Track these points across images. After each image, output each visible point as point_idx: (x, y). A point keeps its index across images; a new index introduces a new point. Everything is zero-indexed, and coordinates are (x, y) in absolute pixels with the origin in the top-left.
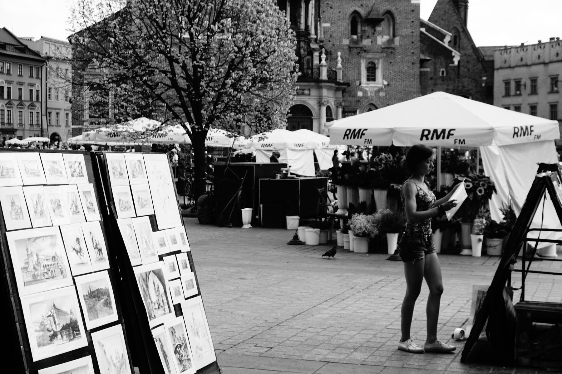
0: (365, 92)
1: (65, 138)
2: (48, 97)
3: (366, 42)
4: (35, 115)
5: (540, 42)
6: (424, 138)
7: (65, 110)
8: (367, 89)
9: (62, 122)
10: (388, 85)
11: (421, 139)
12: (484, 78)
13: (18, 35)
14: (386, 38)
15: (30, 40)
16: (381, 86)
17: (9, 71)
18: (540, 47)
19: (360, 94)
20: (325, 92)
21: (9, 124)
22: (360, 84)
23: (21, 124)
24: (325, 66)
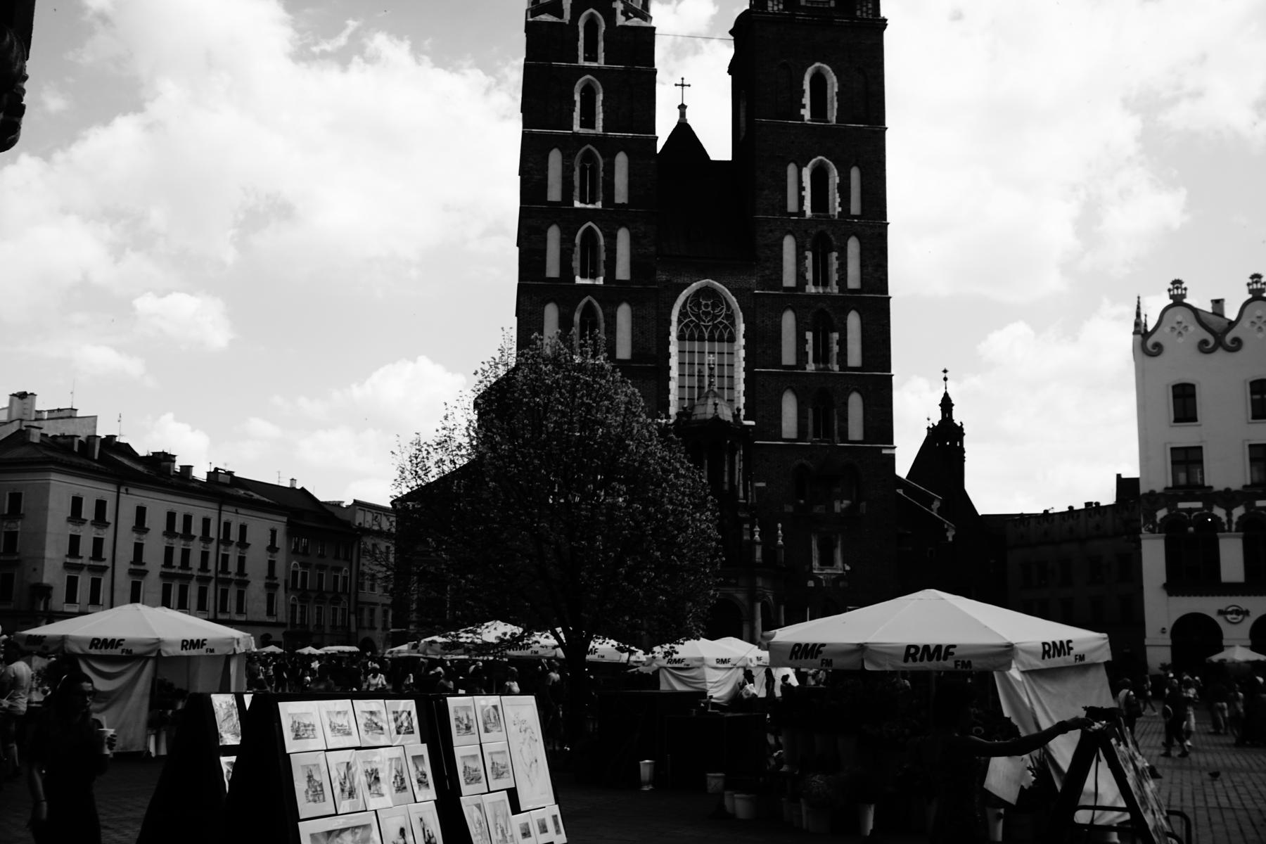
0: (817, 581)
1: (382, 646)
2: (360, 586)
3: (818, 509)
4: (339, 612)
5: (1071, 508)
6: (910, 659)
7: (383, 605)
8: (821, 577)
9: (379, 625)
11: (906, 660)
12: (992, 561)
13: (322, 496)
14: (846, 502)
15: (337, 505)
16: (840, 572)
17: (305, 548)
18: (1073, 517)
19: (811, 584)
20: (760, 582)
21: (302, 624)
22: (811, 568)
23: (319, 626)
24: (759, 544)
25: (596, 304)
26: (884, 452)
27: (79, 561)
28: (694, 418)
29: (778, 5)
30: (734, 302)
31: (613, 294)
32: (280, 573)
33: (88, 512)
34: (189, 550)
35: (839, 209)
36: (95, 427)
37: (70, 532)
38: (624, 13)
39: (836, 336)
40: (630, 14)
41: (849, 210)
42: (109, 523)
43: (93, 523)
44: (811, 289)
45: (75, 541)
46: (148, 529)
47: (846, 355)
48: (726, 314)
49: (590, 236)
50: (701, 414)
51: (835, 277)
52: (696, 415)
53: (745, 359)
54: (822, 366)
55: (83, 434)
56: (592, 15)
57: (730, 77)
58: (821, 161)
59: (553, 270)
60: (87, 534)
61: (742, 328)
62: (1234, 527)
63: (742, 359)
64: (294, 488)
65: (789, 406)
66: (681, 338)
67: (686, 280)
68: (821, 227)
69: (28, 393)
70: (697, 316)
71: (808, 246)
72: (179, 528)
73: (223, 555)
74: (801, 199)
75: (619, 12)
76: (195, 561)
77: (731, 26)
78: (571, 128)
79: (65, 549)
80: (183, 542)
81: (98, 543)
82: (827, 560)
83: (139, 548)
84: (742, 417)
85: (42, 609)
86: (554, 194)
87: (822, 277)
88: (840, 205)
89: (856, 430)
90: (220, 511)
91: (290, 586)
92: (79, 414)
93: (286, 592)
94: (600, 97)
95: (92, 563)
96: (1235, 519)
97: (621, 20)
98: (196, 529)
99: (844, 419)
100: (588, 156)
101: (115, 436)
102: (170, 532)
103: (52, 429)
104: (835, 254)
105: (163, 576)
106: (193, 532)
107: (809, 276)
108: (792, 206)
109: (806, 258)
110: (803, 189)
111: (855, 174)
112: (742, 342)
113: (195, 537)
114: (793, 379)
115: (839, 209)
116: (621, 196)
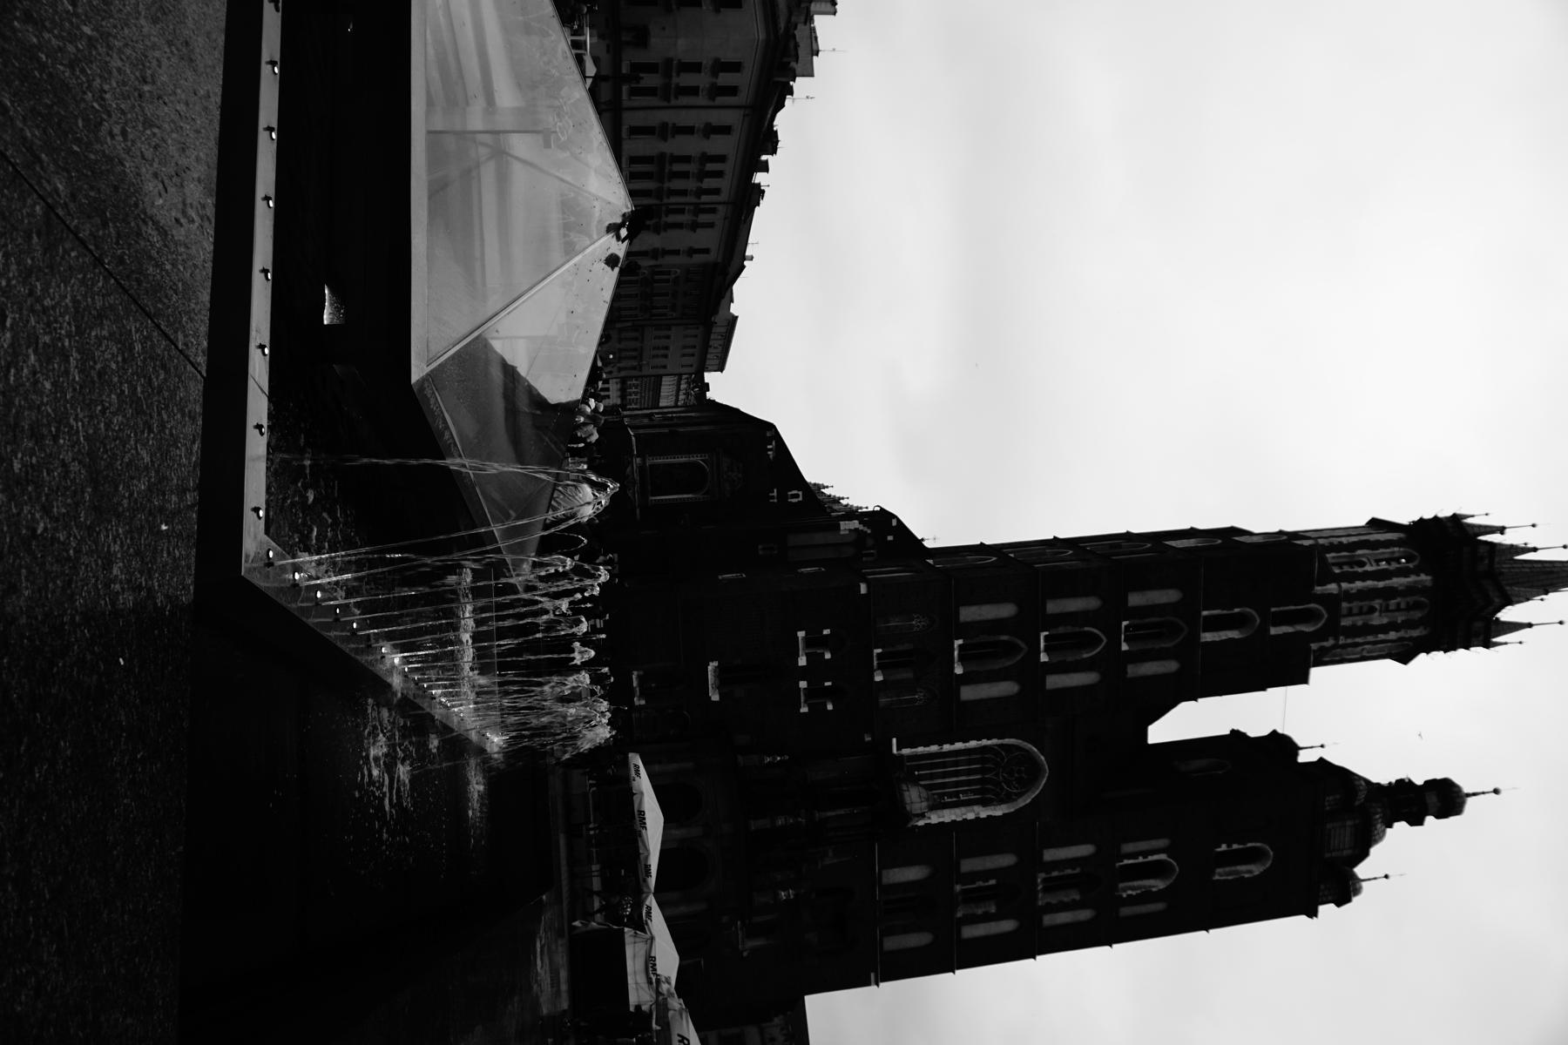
7: (642, 347)
8: (733, 929)
15: (732, 301)
25: (1019, 657)
26: (872, 975)
27: (674, 74)
28: (905, 788)
29: (1329, 805)
30: (1025, 801)
31: (1030, 674)
32: (669, 260)
33: (725, 79)
34: (688, 178)
35: (1125, 895)
36: (803, 76)
37: (704, 62)
39: (993, 910)
42: (714, 100)
43: (713, 85)
44: (1042, 876)
45: (695, 67)
46: (708, 138)
49: (1093, 641)
50: (910, 797)
51: (1053, 899)
52: (908, 790)
53: (964, 819)
54: (960, 898)
55: (798, 67)
57: (1228, 732)
58: (1174, 870)
60: (702, 80)
61: (998, 811)
63: (964, 817)
64: (745, 260)
66: (985, 747)
69: (837, 7)
72: (710, 167)
73: (684, 209)
74: (1134, 855)
76: (677, 184)
77: (1280, 731)
78: (1204, 610)
79: (686, 60)
80: (696, 171)
81: (694, 91)
83: (689, 130)
85: (624, 39)
87: (1052, 886)
88: (1129, 896)
89: (892, 943)
90: (724, 203)
91: (656, 270)
92: (815, 58)
93: (651, 266)
94: (1234, 634)
95: (673, 86)
97: (1314, 646)
98: (709, 183)
99: (906, 930)
101: (792, 94)
102: (706, 158)
103: (800, 33)
104: (1077, 897)
105: (662, 155)
106: (706, 180)
108: (1128, 848)
109: (1074, 869)
110: (1145, 857)
111: (1160, 906)
112: (983, 815)
113: (702, 182)
115: (1125, 895)
116: (1134, 670)
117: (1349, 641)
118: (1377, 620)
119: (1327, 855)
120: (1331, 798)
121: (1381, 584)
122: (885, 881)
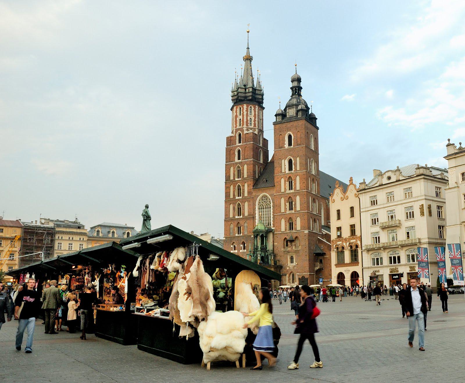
0: (290, 267)
10: (297, 264)
19: (288, 268)
26: (305, 232)
38: (248, 130)
40: (249, 130)
41: (296, 169)
47: (296, 208)
48: (269, 201)
49: (239, 186)
56: (239, 132)
58: (290, 157)
59: (232, 197)
61: (272, 204)
62: (347, 248)
65: (283, 222)
66: (259, 209)
67: (258, 194)
68: (290, 175)
70: (263, 203)
71: (287, 181)
74: (285, 168)
75: (245, 130)
82: (292, 262)
84: (272, 227)
86: (232, 178)
89: (299, 228)
96: (347, 246)
100: (239, 167)
107: (288, 188)
108: (283, 171)
109: (286, 184)
110: (285, 166)
112: (272, 208)
114: (283, 215)
116: (245, 176)
117: (245, 124)
118: (241, 119)
119: (295, 115)
120: (278, 120)
121: (235, 119)
122: (284, 231)
